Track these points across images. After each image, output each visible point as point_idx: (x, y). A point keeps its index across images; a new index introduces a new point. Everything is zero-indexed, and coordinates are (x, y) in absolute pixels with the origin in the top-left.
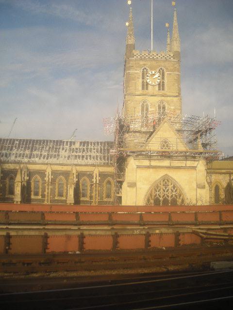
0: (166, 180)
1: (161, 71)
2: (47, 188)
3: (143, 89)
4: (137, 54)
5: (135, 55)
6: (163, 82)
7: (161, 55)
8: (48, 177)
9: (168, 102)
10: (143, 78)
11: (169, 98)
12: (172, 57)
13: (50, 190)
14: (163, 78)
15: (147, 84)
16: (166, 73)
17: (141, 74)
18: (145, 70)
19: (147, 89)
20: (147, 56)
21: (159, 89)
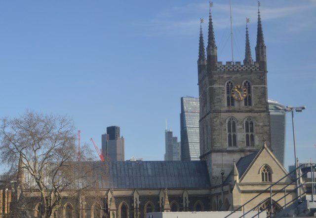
2: (135, 214)
3: (228, 104)
4: (221, 67)
5: (219, 68)
6: (250, 97)
7: (246, 67)
8: (136, 202)
9: (255, 118)
10: (228, 92)
11: (256, 114)
12: (258, 68)
13: (138, 216)
14: (249, 92)
15: (233, 99)
17: (226, 89)
18: (230, 84)
19: (233, 105)
20: (231, 68)
21: (246, 104)
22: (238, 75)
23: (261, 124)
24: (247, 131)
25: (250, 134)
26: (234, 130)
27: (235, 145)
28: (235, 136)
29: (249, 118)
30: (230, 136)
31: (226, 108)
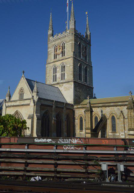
1: (63, 44)
18: (56, 47)
21: (62, 56)
23: (68, 65)
24: (62, 71)
25: (63, 73)
26: (56, 73)
27: (56, 80)
28: (56, 75)
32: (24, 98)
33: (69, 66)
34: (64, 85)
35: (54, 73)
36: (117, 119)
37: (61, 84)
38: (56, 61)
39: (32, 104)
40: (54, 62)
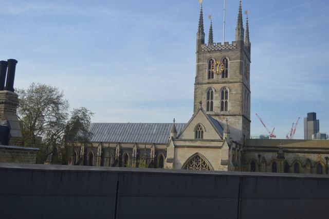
0: (196, 157)
3: (209, 78)
6: (227, 71)
10: (209, 68)
11: (230, 84)
14: (227, 67)
16: (229, 62)
18: (211, 62)
19: (212, 78)
21: (223, 77)
22: (218, 54)
24: (222, 98)
25: (224, 101)
26: (212, 98)
27: (212, 110)
28: (212, 102)
29: (224, 88)
30: (208, 103)
31: (207, 81)
32: (206, 136)
33: (235, 94)
34: (228, 117)
35: (208, 99)
36: (302, 167)
37: (222, 117)
38: (214, 83)
39: (226, 147)
40: (209, 83)
